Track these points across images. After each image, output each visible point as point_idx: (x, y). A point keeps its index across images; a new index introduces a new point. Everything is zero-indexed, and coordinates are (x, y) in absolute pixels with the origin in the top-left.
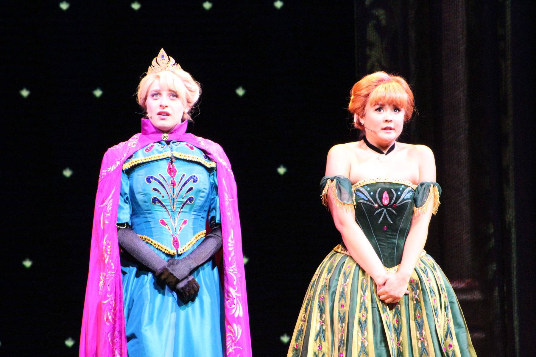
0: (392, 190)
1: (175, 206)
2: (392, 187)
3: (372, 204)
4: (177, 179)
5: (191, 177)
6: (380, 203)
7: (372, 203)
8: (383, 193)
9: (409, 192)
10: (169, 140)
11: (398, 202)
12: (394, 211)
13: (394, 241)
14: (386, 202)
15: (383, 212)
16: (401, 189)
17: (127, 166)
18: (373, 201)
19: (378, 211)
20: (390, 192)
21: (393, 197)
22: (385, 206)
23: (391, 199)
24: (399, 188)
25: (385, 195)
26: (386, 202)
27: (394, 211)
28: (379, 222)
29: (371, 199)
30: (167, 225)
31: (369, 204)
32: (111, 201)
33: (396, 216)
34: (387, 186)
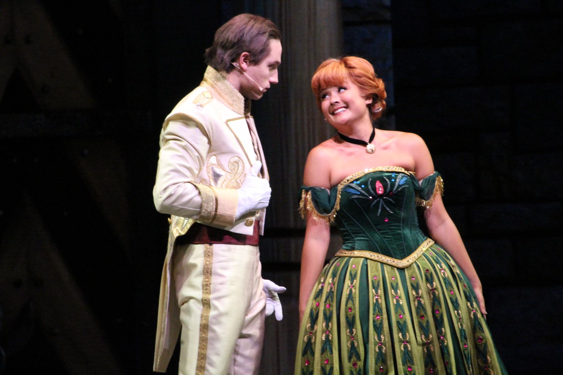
12: (391, 200)
14: (380, 191)
19: (374, 203)
22: (381, 196)
23: (385, 187)
25: (378, 185)
26: (380, 191)
27: (391, 200)
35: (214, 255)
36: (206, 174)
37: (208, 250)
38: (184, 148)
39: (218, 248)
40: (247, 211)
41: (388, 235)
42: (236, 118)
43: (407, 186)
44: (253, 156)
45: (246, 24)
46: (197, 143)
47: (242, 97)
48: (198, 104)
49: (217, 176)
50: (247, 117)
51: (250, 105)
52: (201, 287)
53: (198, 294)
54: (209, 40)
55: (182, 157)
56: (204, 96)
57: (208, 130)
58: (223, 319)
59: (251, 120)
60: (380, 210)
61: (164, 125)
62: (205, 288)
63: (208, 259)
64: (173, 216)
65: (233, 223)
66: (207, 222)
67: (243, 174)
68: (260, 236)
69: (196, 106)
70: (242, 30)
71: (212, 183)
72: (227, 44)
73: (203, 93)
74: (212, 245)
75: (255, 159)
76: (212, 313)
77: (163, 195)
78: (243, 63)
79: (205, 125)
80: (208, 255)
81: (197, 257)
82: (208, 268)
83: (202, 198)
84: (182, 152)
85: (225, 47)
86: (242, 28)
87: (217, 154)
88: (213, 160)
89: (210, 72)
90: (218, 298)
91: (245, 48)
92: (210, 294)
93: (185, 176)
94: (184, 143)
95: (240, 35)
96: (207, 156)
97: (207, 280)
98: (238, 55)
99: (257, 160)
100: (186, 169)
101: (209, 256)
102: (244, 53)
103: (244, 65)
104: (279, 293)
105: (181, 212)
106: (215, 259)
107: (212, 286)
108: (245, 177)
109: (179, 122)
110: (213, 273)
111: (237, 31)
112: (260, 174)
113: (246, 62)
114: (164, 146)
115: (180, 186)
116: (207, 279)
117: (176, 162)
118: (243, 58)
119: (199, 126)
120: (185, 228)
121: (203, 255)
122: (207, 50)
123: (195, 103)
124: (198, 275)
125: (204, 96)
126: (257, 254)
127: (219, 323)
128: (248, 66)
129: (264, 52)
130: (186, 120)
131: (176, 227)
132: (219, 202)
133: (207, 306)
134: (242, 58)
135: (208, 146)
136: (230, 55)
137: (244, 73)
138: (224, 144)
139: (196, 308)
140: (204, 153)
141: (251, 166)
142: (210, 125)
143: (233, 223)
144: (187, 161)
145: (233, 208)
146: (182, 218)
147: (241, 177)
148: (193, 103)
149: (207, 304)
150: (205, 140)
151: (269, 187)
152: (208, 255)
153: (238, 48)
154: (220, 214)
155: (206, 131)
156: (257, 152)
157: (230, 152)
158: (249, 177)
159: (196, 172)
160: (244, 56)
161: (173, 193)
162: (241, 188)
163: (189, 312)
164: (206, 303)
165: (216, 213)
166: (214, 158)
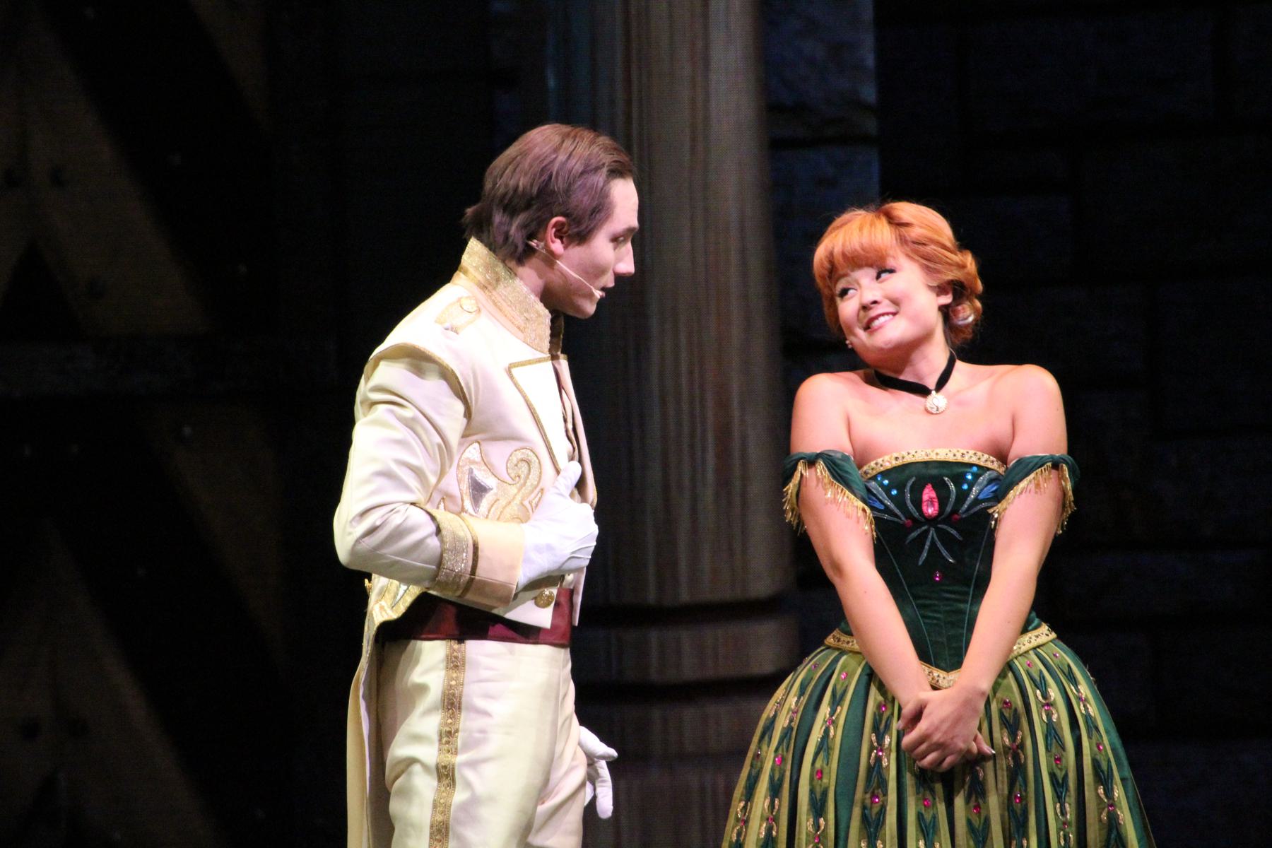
0: (946, 479)
2: (945, 471)
3: (896, 519)
6: (916, 515)
12: (953, 532)
13: (962, 606)
16: (969, 477)
18: (897, 511)
19: (914, 534)
20: (940, 486)
21: (949, 497)
22: (931, 521)
23: (943, 501)
25: (928, 493)
26: (931, 511)
27: (953, 532)
28: (920, 563)
29: (892, 506)
34: (934, 472)
35: (467, 667)
36: (455, 484)
37: (455, 654)
38: (409, 424)
39: (481, 651)
40: (542, 573)
42: (530, 360)
44: (562, 447)
45: (556, 150)
46: (440, 414)
47: (547, 311)
48: (447, 325)
49: (478, 490)
50: (554, 357)
51: (563, 331)
52: (435, 737)
53: (429, 753)
54: (474, 191)
55: (400, 443)
56: (461, 307)
57: (469, 388)
58: (484, 812)
59: (564, 365)
60: (925, 554)
61: (367, 368)
62: (444, 740)
63: (454, 675)
64: (374, 576)
65: (512, 598)
66: (449, 595)
67: (538, 489)
68: (573, 628)
69: (443, 330)
70: (546, 166)
71: (468, 504)
72: (516, 201)
73: (459, 300)
74: (463, 643)
75: (566, 458)
76: (459, 796)
77: (355, 527)
78: (553, 242)
79: (462, 374)
80: (455, 664)
81: (426, 671)
82: (454, 695)
83: (442, 542)
84: (403, 433)
85: (512, 205)
86: (546, 162)
87: (485, 440)
88: (473, 452)
89: (475, 253)
90: (473, 764)
91: (556, 209)
92: (456, 754)
93: (407, 488)
94: (409, 412)
95: (543, 178)
96: (461, 444)
97: (450, 721)
98: (542, 223)
99: (571, 459)
100: (410, 471)
101: (457, 666)
102: (555, 220)
103: (557, 246)
104: (609, 760)
105: (394, 570)
106: (469, 675)
107: (460, 735)
108: (542, 493)
109: (403, 362)
110: (463, 706)
111: (536, 168)
112: (576, 492)
113: (561, 238)
114: (365, 416)
115: (395, 510)
116: (451, 718)
117: (390, 456)
118: (554, 230)
119: (447, 375)
120: (401, 603)
121: (443, 665)
122: (469, 211)
123: (441, 323)
124: (428, 712)
125: (461, 307)
126: (564, 666)
127: (474, 820)
128: (565, 248)
129: (599, 211)
130: (418, 360)
131: (380, 601)
132: (480, 553)
133: (447, 781)
134: (551, 232)
135: (465, 421)
136: (524, 226)
137: (558, 262)
138: (501, 418)
139: (424, 785)
140: (454, 437)
141: (558, 472)
142: (471, 376)
143: (512, 598)
144: (414, 453)
145: (512, 568)
146: (396, 582)
147: (533, 496)
148: (436, 322)
149: (447, 776)
150: (459, 407)
151: (594, 522)
152: (455, 664)
153: (539, 209)
154: (480, 580)
155: (462, 388)
156: (572, 436)
157: (513, 437)
158: (550, 497)
159: (433, 480)
160: (555, 226)
161: (378, 523)
162: (531, 522)
163: (407, 793)
164: (445, 774)
165: (472, 577)
166: (475, 449)
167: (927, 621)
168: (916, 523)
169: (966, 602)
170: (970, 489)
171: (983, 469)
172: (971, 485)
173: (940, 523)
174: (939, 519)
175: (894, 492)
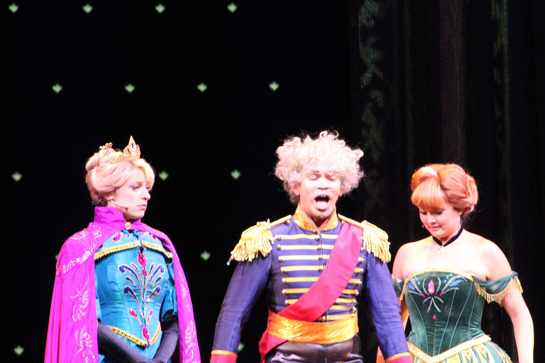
0: (438, 278)
1: (145, 296)
2: (439, 275)
3: (416, 293)
4: (147, 269)
5: (159, 267)
6: (426, 292)
7: (419, 292)
8: (429, 282)
9: (457, 279)
10: (131, 229)
11: (443, 290)
12: (441, 300)
13: (442, 330)
14: (431, 290)
15: (430, 302)
16: (447, 277)
17: (97, 256)
18: (420, 292)
19: (425, 300)
20: (435, 280)
21: (438, 285)
22: (432, 295)
23: (436, 287)
24: (446, 277)
25: (431, 284)
26: (431, 290)
27: (441, 300)
28: (428, 312)
29: (418, 289)
30: (136, 315)
31: (416, 293)
32: (86, 292)
33: (444, 305)
34: (434, 275)
41: (431, 332)
43: (457, 288)
60: (429, 308)
167: (428, 336)
168: (427, 296)
169: (444, 328)
170: (447, 283)
171: (455, 275)
172: (447, 281)
173: (435, 296)
174: (435, 294)
175: (419, 283)
